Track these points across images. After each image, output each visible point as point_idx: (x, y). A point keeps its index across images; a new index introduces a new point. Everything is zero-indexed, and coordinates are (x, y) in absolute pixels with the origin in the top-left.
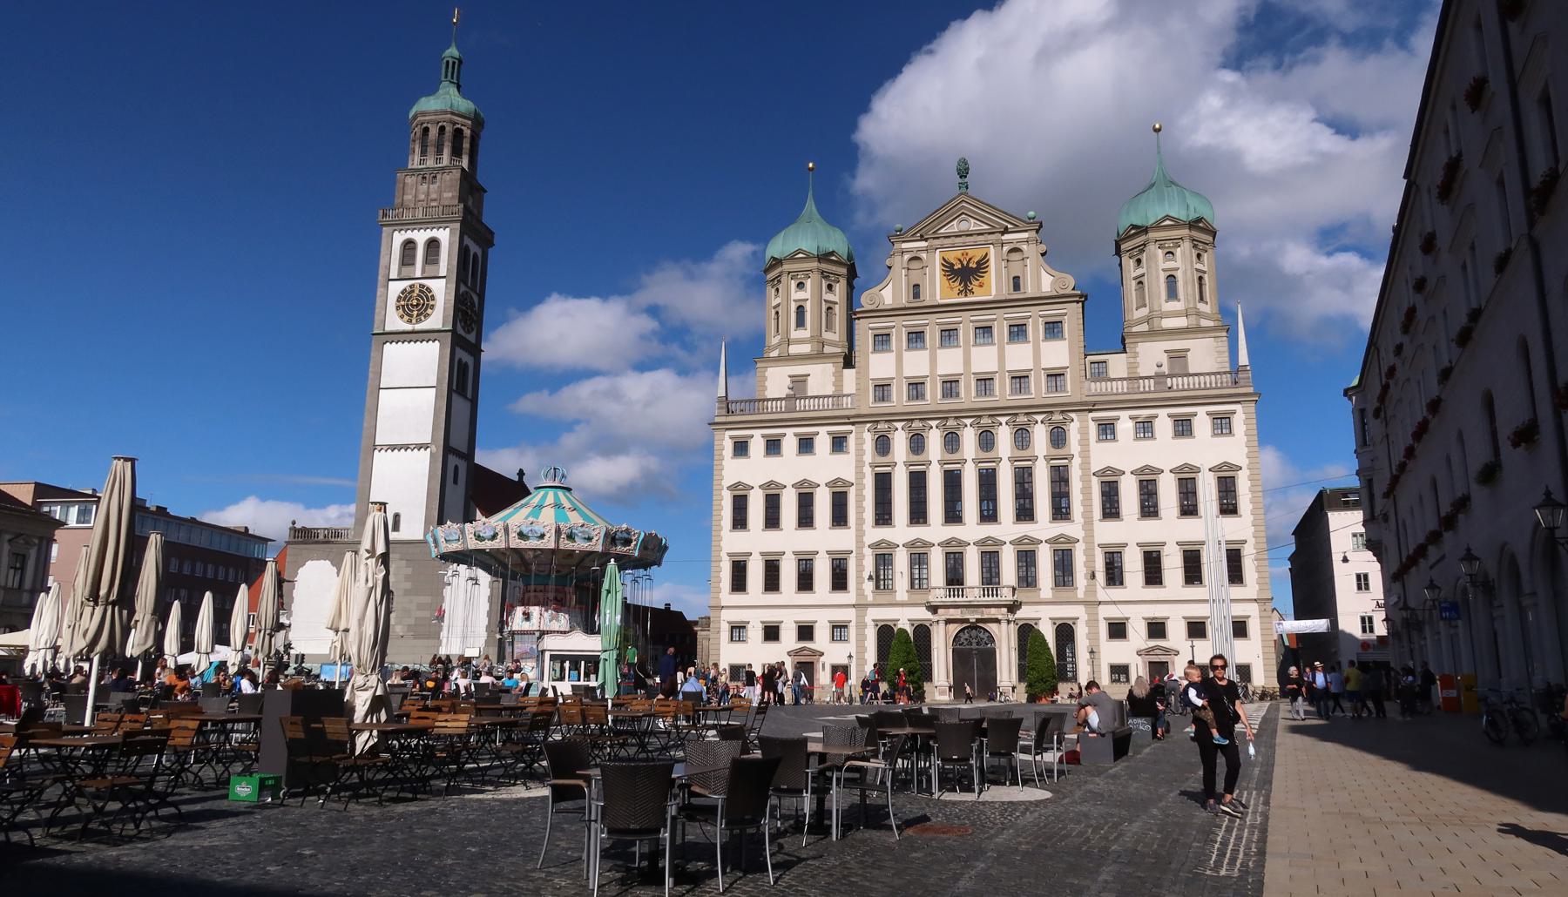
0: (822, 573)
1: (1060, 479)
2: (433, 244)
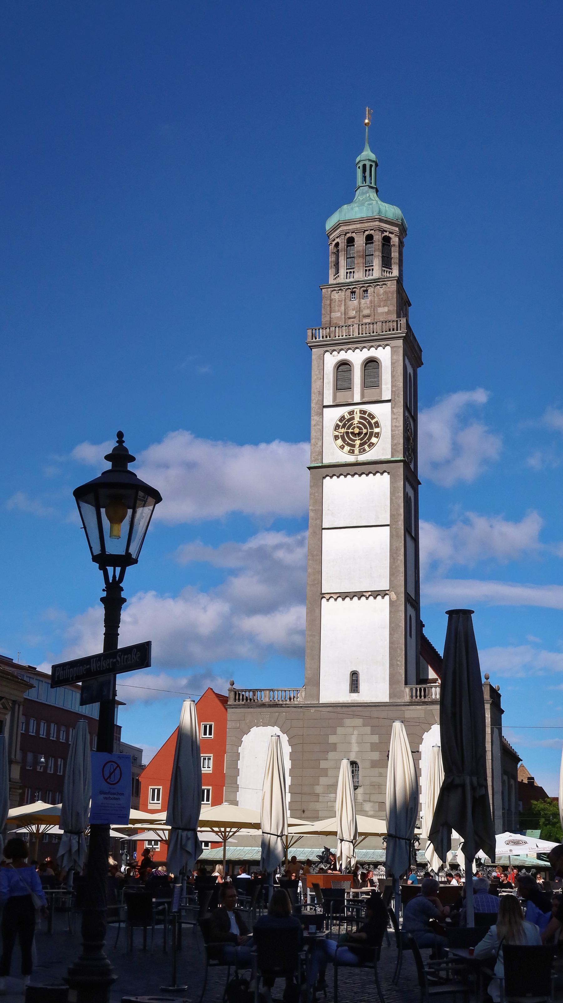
2: (371, 364)
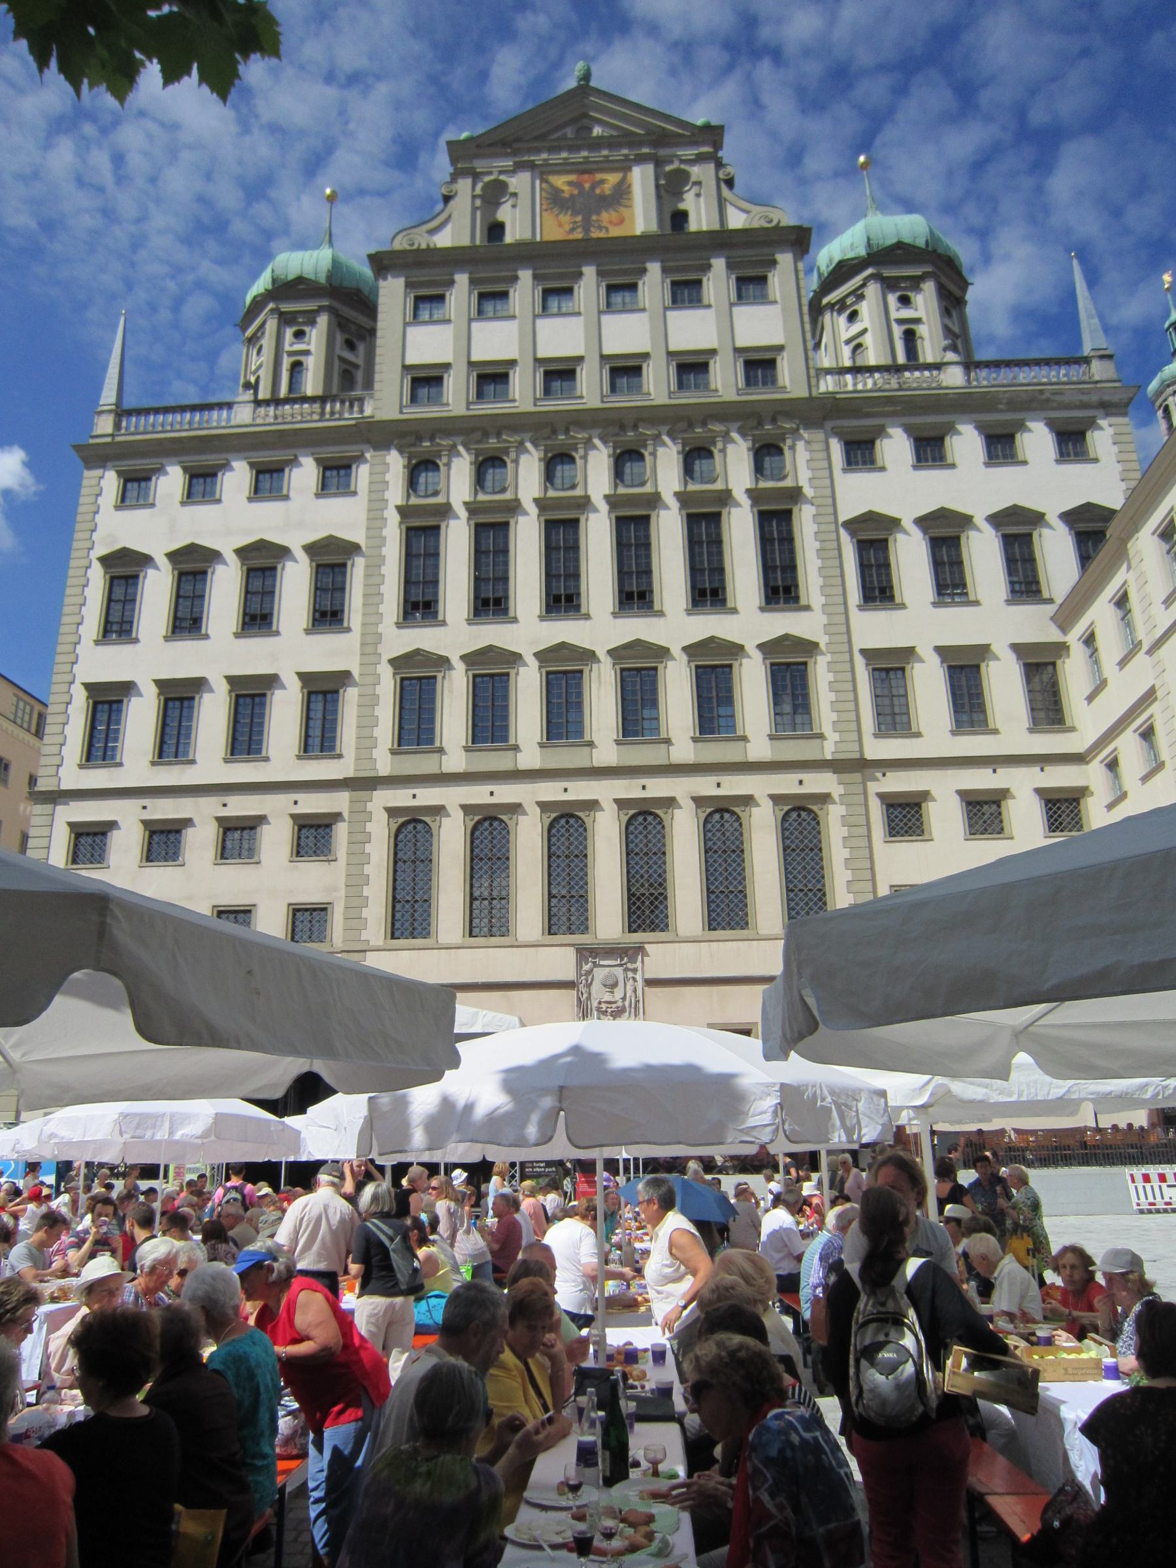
0: (285, 715)
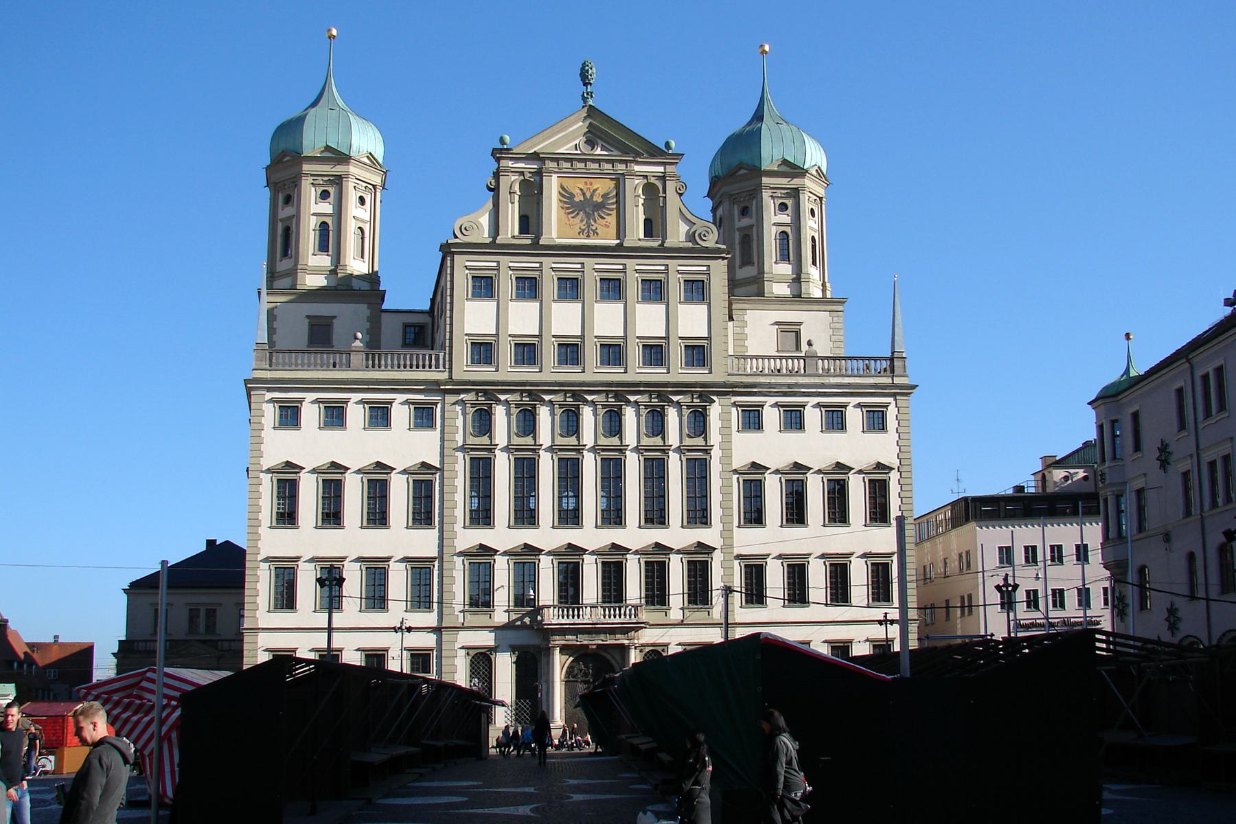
0: (398, 583)
1: (698, 473)
